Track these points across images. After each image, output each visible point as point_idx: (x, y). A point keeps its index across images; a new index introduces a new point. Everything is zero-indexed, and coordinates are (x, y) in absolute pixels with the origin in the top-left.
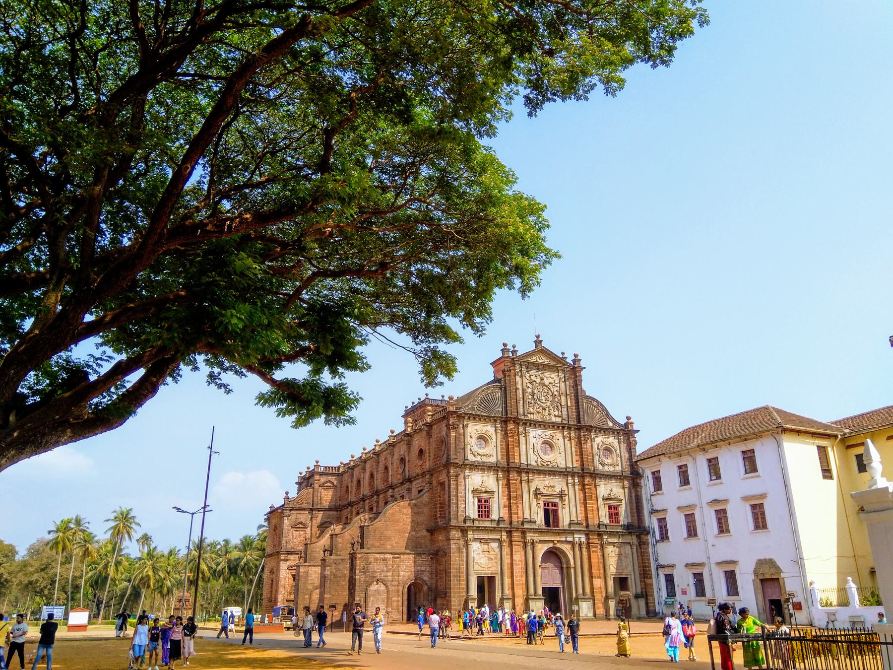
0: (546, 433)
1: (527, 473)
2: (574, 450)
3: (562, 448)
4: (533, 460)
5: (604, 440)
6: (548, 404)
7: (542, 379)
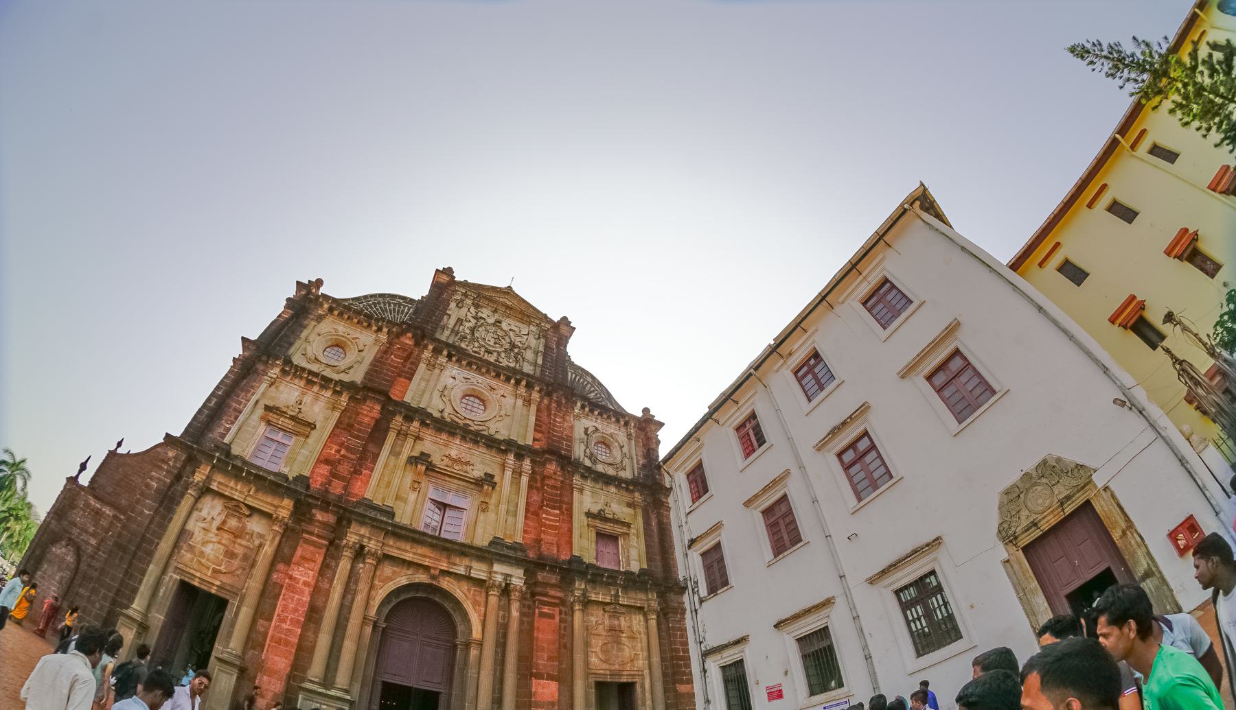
0: (481, 382)
1: (408, 419)
2: (532, 418)
4: (435, 405)
5: (599, 427)
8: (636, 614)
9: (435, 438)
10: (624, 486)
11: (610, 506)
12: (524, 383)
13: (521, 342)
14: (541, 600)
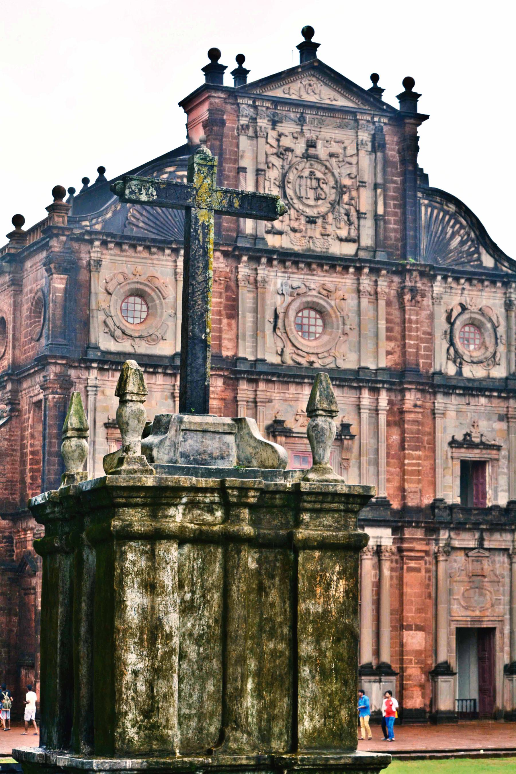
2: (382, 324)
3: (352, 320)
6: (323, 207)
7: (311, 144)
8: (499, 555)
9: (282, 395)
10: (495, 394)
11: (478, 426)
12: (366, 270)
13: (349, 174)
14: (408, 556)
